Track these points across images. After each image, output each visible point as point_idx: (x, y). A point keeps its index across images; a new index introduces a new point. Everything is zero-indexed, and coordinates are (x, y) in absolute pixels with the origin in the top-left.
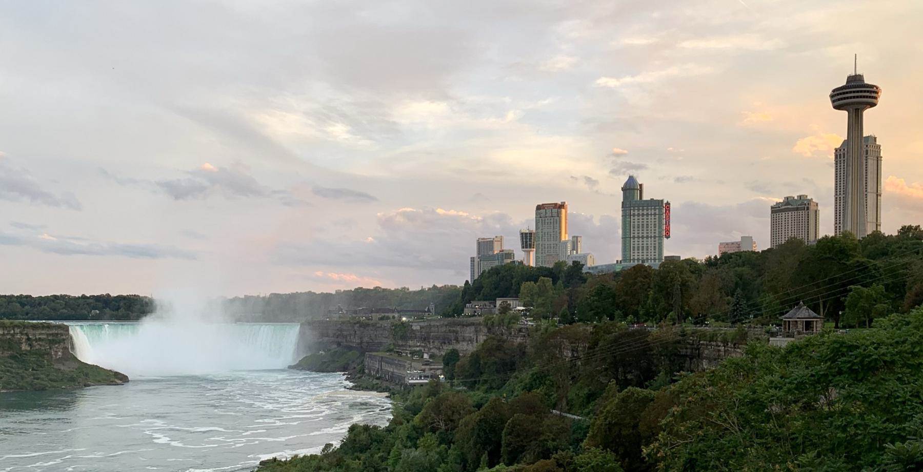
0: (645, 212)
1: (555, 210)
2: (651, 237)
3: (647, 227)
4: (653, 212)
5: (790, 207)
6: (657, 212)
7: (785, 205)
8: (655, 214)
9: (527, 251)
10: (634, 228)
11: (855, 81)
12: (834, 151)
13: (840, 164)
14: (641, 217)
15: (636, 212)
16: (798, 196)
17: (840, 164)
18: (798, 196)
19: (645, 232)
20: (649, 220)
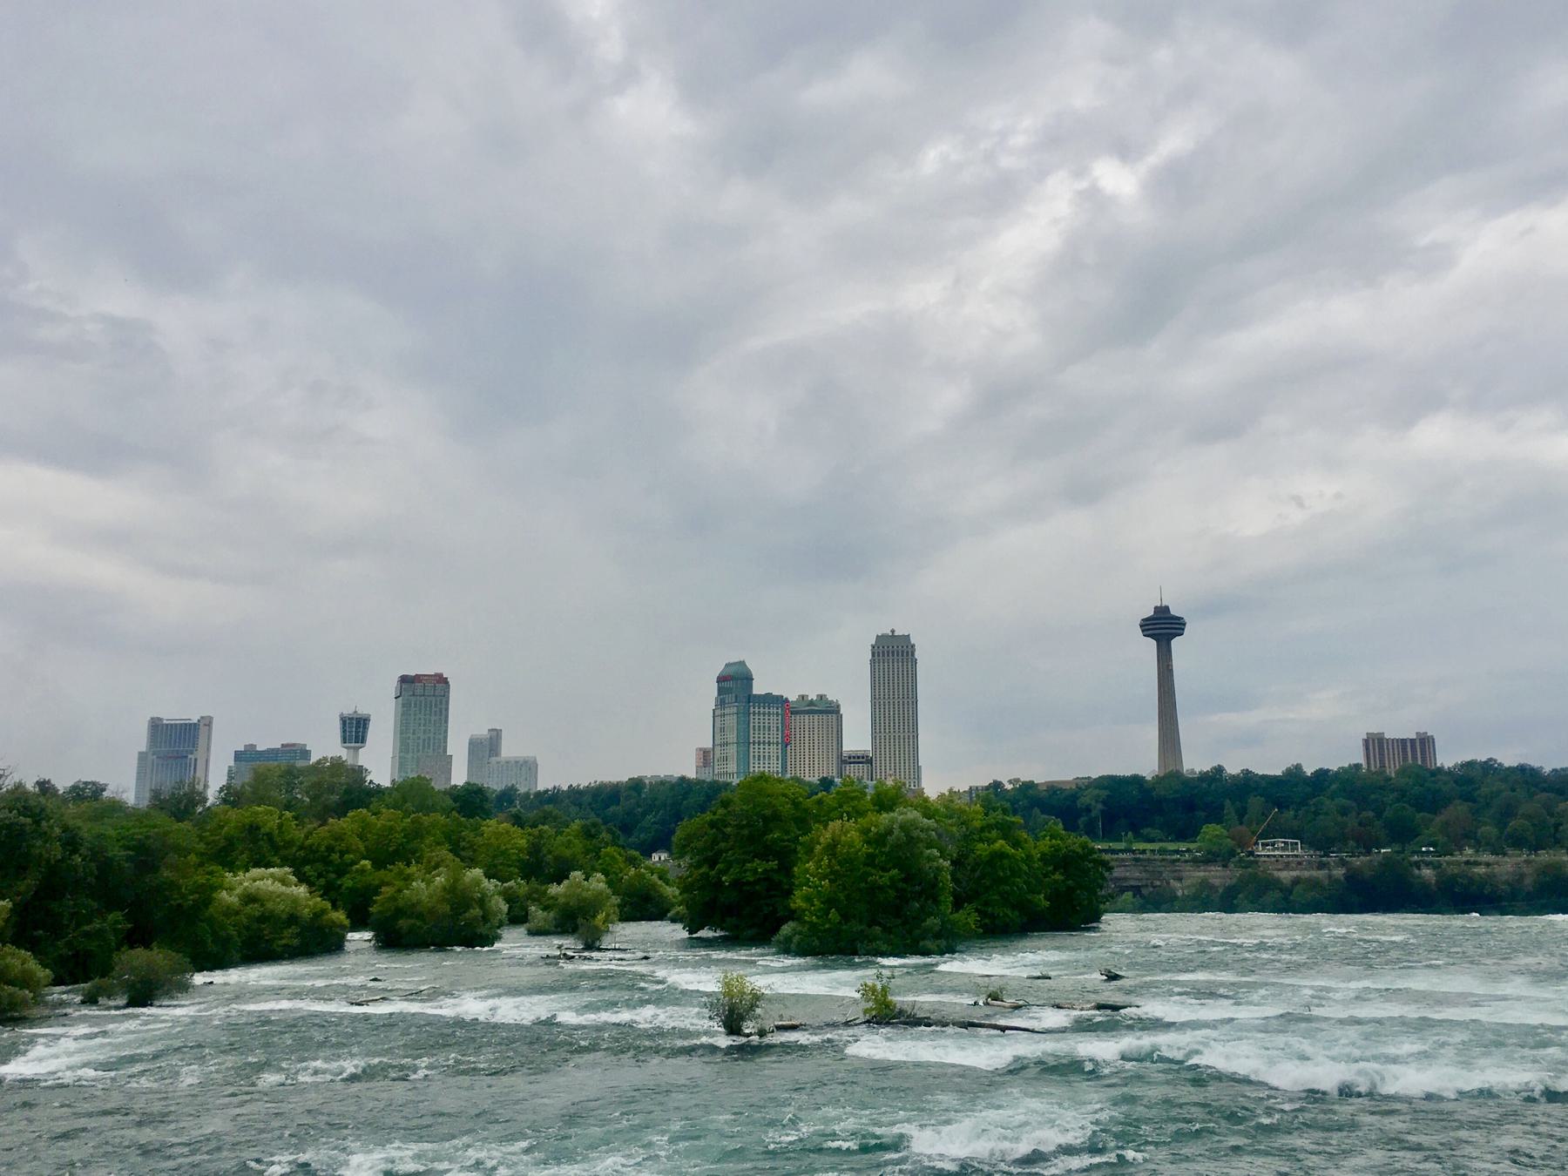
0: (767, 710)
1: (439, 686)
2: (773, 743)
3: (769, 730)
4: (775, 711)
5: (816, 708)
6: (780, 711)
7: (808, 706)
8: (777, 714)
9: (354, 748)
10: (754, 730)
11: (1162, 613)
12: (870, 648)
13: (903, 662)
14: (762, 717)
15: (757, 710)
16: (818, 696)
17: (903, 662)
18: (818, 696)
19: (767, 736)
20: (771, 721)
